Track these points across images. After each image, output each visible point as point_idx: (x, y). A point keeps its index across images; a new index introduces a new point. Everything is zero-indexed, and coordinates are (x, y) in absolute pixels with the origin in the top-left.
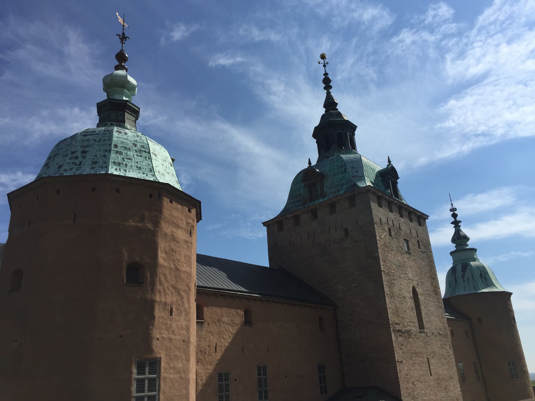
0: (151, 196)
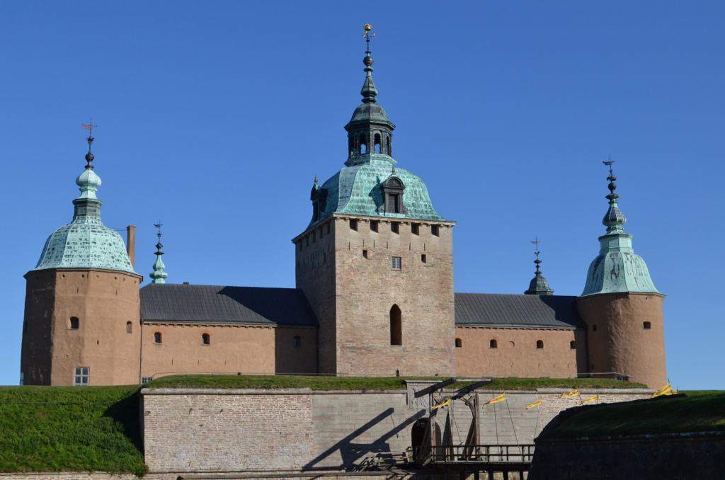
0: (83, 276)
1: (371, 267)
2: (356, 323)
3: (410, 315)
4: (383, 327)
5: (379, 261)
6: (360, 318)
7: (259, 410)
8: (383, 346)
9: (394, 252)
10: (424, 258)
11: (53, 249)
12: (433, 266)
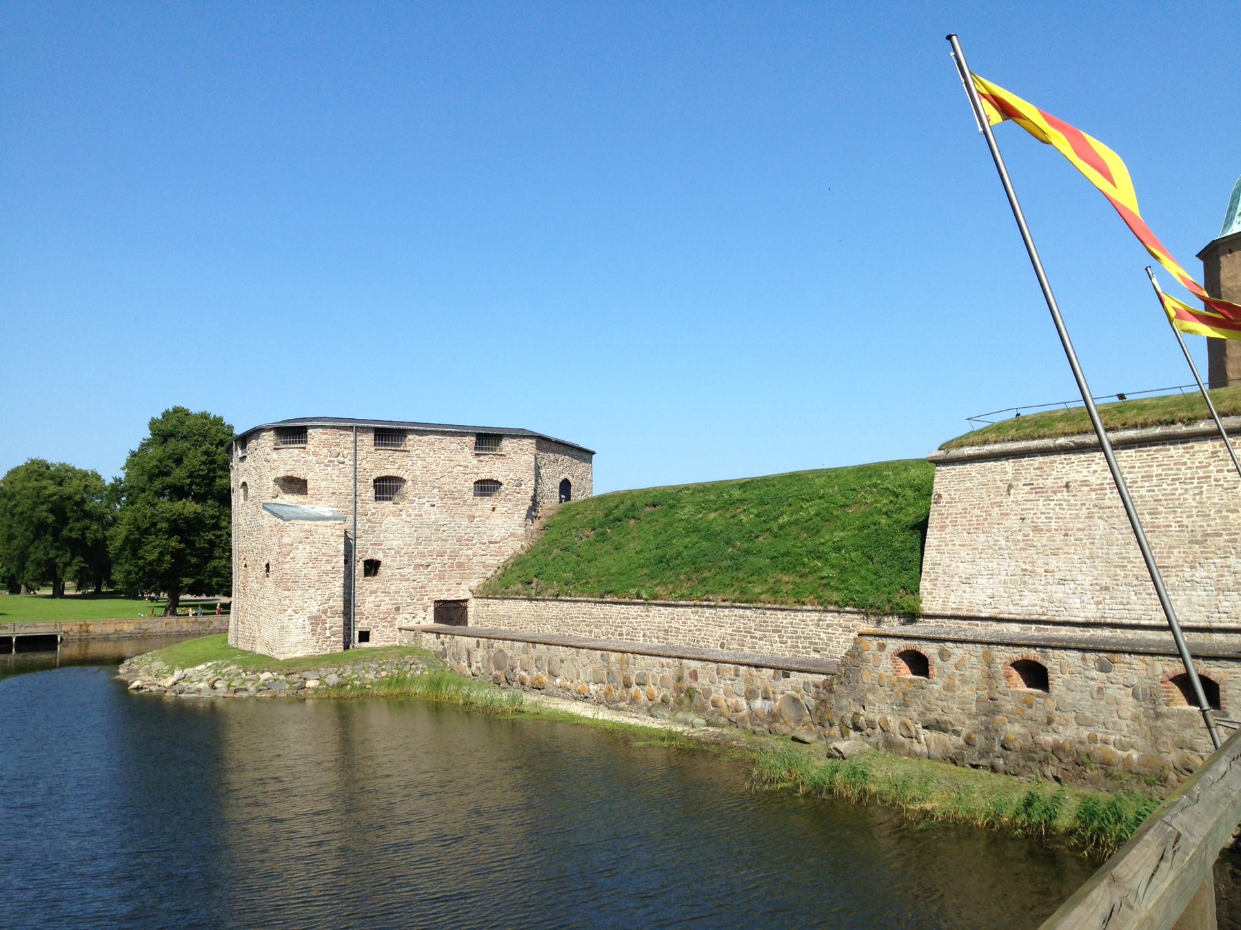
7: (1148, 477)
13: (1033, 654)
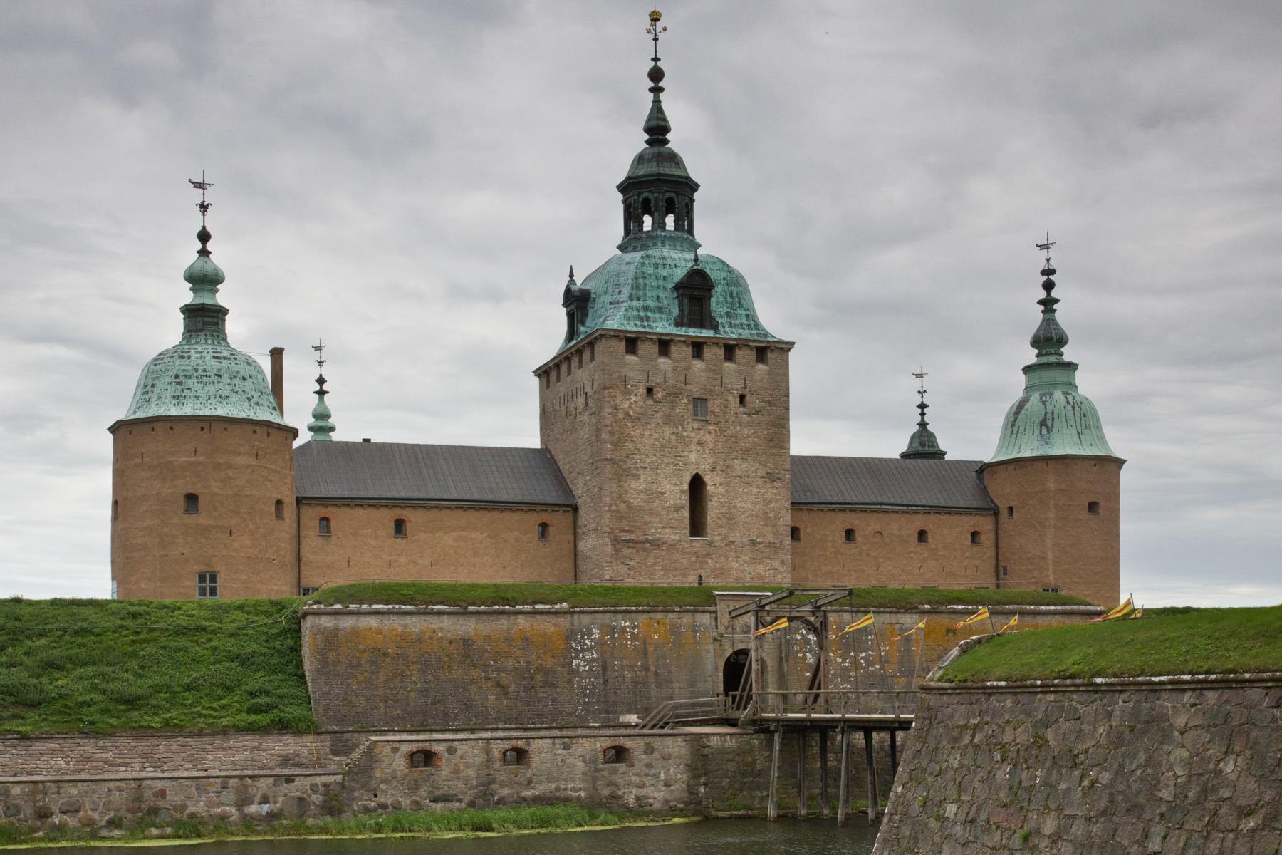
1: (660, 414)
2: (635, 503)
3: (721, 490)
4: (678, 509)
5: (673, 404)
6: (642, 496)
8: (676, 537)
9: (695, 390)
10: (742, 398)
11: (153, 386)
12: (757, 413)
13: (521, 743)
